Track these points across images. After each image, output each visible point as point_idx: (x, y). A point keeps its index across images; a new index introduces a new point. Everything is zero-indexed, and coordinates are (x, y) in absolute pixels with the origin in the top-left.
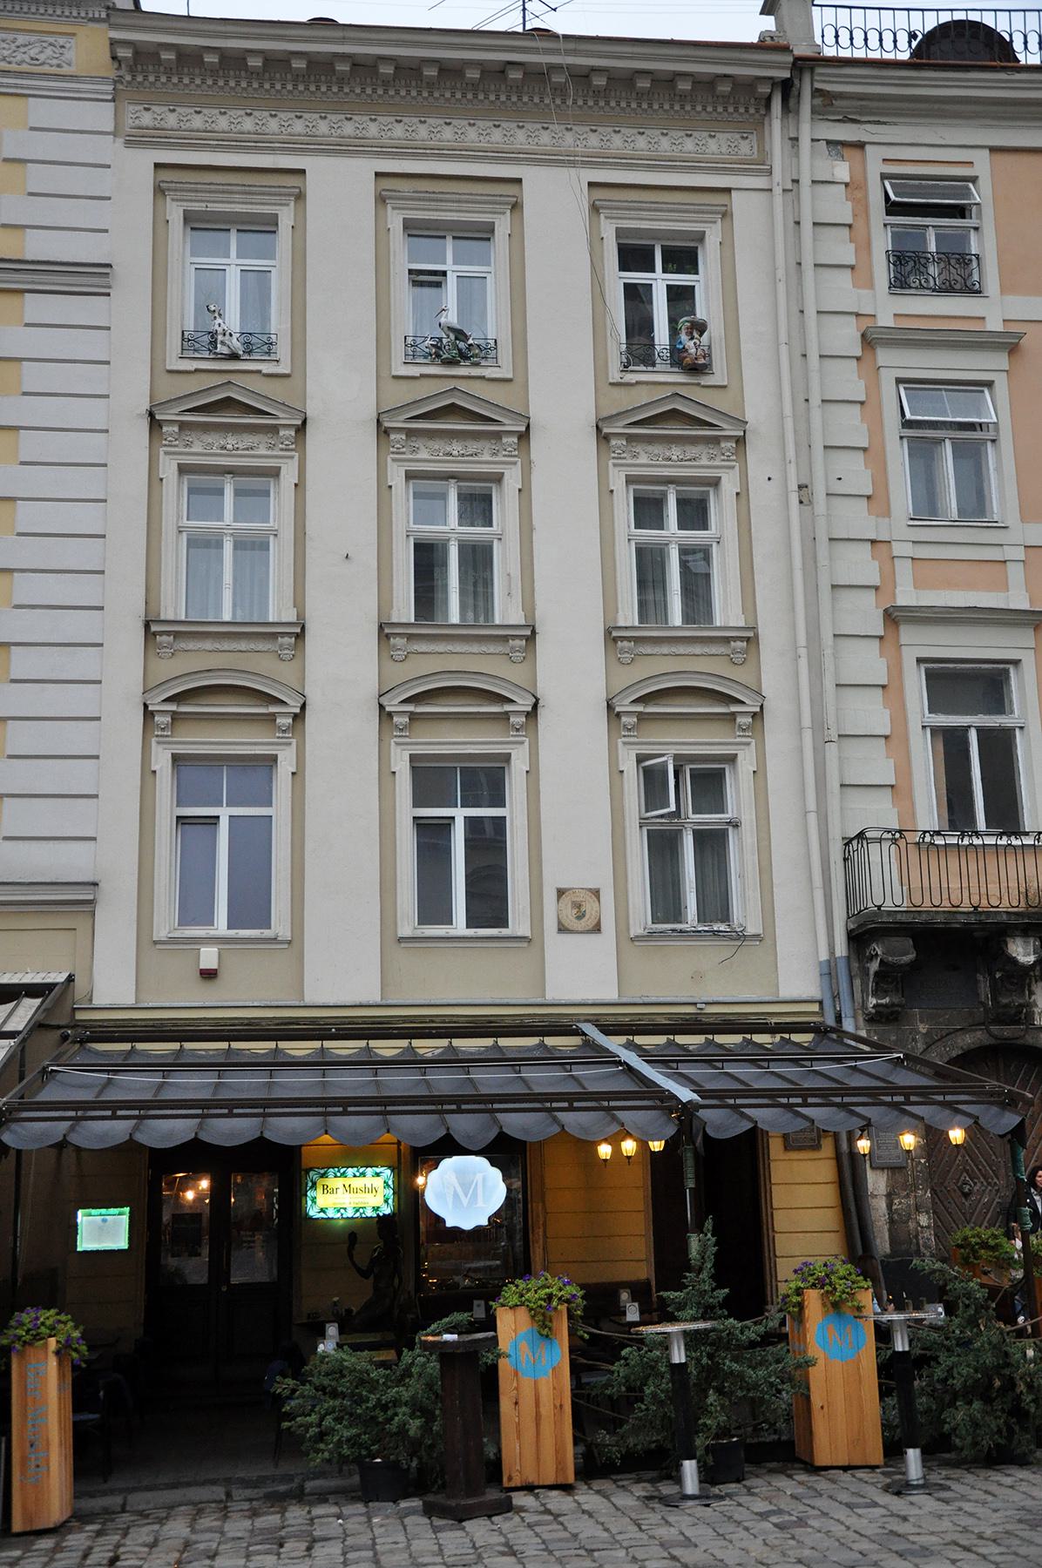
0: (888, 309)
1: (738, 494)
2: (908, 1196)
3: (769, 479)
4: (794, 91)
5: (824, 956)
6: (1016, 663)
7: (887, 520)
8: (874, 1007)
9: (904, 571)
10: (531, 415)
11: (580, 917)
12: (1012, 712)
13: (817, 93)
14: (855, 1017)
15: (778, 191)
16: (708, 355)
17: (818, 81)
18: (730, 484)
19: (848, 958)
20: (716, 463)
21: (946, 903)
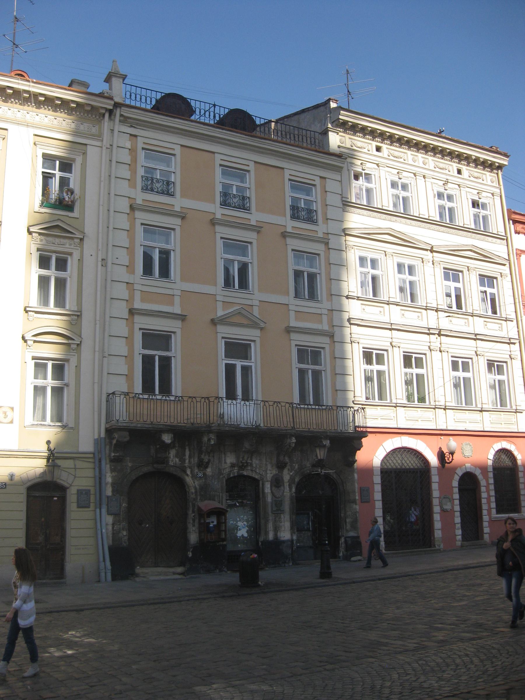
0: (140, 197)
1: (79, 260)
2: (120, 525)
3: (91, 255)
4: (114, 114)
5: (96, 437)
6: (174, 333)
7: (133, 275)
8: (113, 456)
9: (138, 295)
10: (2, 221)
11: (5, 418)
12: (171, 351)
13: (121, 115)
14: (106, 460)
15: (104, 148)
16: (73, 202)
17: (122, 112)
18: (76, 255)
19: (105, 438)
20: (72, 247)
21: (141, 420)
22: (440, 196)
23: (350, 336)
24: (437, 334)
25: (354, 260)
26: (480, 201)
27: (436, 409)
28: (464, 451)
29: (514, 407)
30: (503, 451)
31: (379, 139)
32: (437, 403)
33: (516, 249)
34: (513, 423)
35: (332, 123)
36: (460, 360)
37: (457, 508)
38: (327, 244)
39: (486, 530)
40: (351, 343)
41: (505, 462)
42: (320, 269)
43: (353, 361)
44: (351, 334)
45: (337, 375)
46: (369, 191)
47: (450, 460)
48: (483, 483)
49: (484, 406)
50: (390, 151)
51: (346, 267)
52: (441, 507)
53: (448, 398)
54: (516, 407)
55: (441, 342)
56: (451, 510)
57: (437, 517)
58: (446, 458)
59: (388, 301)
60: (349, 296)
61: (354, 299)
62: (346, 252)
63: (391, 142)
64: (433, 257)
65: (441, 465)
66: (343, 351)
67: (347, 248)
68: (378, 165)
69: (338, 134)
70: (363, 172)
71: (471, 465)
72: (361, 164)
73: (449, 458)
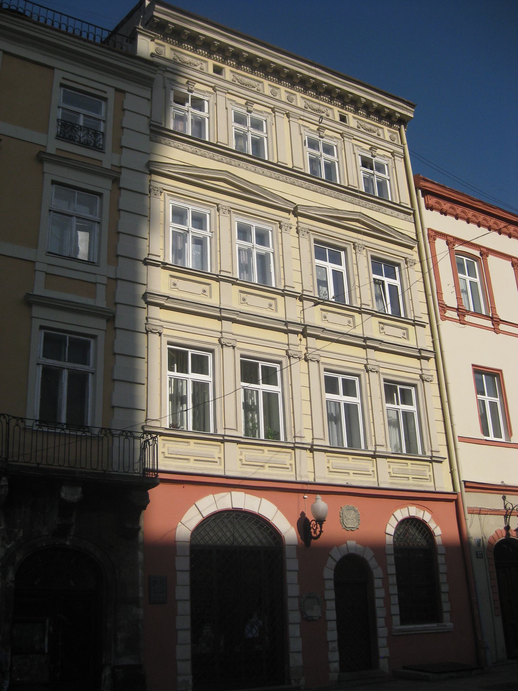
22: (313, 144)
23: (145, 321)
24: (302, 333)
25: (162, 209)
26: (374, 159)
27: (297, 451)
28: (344, 520)
29: (429, 454)
30: (412, 522)
31: (219, 56)
32: (298, 440)
33: (428, 229)
34: (428, 477)
35: (145, 25)
36: (340, 377)
37: (332, 615)
38: (116, 180)
39: (384, 652)
40: (147, 333)
41: (416, 539)
42: (101, 216)
43: (147, 362)
44: (147, 319)
45: (116, 382)
46: (199, 124)
47: (318, 533)
48: (377, 572)
49: (379, 449)
50: (237, 76)
51: (147, 219)
52: (302, 613)
53: (318, 434)
54: (432, 454)
55: (307, 345)
56: (320, 617)
57: (294, 631)
58: (312, 530)
59: (217, 275)
60: (147, 261)
61: (158, 266)
62: (150, 197)
63: (237, 63)
64: (297, 223)
65: (303, 543)
66: (134, 345)
67: (153, 191)
68: (214, 88)
69: (153, 40)
70: (190, 94)
71: (357, 543)
72: (187, 83)
73: (316, 529)
